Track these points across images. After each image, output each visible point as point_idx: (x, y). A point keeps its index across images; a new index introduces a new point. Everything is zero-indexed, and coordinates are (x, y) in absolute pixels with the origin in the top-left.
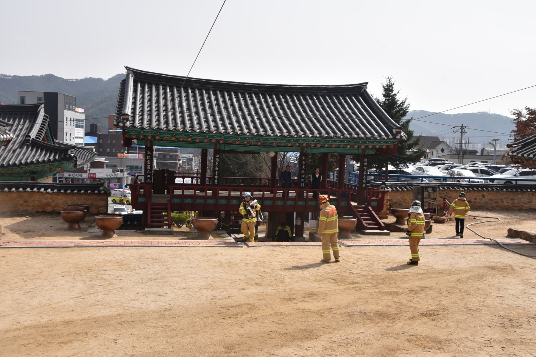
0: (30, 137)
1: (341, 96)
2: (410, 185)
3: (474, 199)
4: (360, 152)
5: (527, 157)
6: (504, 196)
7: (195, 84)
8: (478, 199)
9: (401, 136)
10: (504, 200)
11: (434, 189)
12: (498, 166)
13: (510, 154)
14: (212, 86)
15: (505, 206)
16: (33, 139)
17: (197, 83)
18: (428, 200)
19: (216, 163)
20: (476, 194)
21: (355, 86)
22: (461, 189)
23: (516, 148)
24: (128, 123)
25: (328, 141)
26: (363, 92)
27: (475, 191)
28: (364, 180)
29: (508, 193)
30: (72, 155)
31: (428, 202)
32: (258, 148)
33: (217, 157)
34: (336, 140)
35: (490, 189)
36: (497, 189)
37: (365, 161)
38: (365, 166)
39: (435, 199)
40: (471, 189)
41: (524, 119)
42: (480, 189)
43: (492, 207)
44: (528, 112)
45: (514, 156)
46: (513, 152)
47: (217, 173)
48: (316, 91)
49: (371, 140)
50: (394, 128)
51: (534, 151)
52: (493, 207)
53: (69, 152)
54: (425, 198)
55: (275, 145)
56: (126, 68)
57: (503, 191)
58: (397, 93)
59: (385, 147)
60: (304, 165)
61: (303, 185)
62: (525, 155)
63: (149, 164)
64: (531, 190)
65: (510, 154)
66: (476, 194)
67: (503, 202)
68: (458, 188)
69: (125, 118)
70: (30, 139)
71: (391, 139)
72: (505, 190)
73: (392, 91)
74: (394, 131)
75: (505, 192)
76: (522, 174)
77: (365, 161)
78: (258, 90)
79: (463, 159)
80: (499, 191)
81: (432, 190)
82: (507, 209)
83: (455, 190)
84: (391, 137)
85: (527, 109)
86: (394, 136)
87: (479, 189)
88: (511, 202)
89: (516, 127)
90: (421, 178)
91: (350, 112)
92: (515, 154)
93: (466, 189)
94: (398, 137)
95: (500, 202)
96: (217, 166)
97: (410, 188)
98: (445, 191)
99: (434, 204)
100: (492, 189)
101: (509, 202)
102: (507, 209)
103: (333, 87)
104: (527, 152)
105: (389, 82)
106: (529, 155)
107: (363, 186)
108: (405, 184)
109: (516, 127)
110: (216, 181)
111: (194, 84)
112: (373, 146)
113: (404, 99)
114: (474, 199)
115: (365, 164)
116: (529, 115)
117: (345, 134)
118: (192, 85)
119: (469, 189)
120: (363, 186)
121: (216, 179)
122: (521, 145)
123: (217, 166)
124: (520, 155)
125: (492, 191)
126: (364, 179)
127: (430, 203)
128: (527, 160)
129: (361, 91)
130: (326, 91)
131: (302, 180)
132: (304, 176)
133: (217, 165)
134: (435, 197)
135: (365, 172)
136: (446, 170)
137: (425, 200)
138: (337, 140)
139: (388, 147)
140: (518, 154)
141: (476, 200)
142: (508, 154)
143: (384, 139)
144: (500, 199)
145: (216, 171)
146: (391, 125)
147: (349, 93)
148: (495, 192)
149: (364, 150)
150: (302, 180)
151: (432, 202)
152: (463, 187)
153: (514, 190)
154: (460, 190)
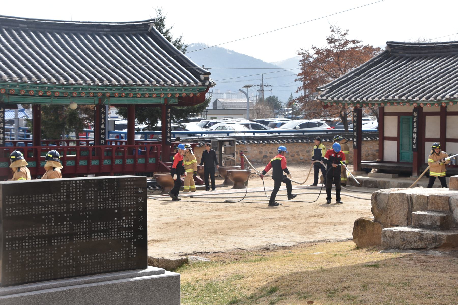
1: (119, 35)
2: (202, 141)
3: (270, 153)
4: (162, 102)
5: (337, 100)
6: (300, 148)
8: (274, 153)
9: (210, 82)
10: (300, 153)
11: (231, 142)
12: (266, 120)
13: (320, 98)
15: (301, 160)
18: (226, 156)
20: (272, 148)
21: (141, 23)
22: (256, 142)
23: (324, 92)
25: (135, 89)
26: (150, 30)
27: (270, 143)
28: (169, 133)
29: (303, 144)
31: (226, 158)
32: (49, 100)
34: (143, 88)
35: (286, 141)
36: (292, 141)
37: (168, 112)
38: (168, 117)
39: (234, 154)
40: (266, 142)
41: (311, 60)
42: (276, 141)
43: (288, 161)
44: (315, 52)
45: (323, 99)
46: (322, 96)
48: (97, 30)
49: (180, 88)
50: (201, 74)
51: (342, 94)
52: (290, 161)
54: (223, 154)
55: (85, 96)
57: (299, 143)
58: (170, 29)
59: (191, 95)
60: (103, 118)
61: (104, 142)
62: (335, 99)
64: (326, 140)
65: (320, 98)
66: (272, 147)
67: (298, 155)
68: (253, 142)
71: (200, 86)
72: (300, 141)
73: (163, 26)
74: (202, 77)
75: (300, 144)
76: (302, 126)
77: (168, 112)
78: (26, 26)
79: (207, 115)
80: (294, 142)
81: (230, 144)
82: (303, 162)
83: (251, 144)
84: (200, 83)
85: (313, 48)
86: (203, 82)
87: (274, 142)
88: (307, 154)
89: (302, 69)
90: (200, 135)
91: (145, 56)
92: (324, 98)
93: (261, 142)
94: (207, 84)
95: (296, 156)
97: (203, 144)
98: (240, 145)
99: (233, 159)
100: (288, 141)
101: (304, 154)
102: (303, 162)
103: (117, 24)
104: (336, 95)
105: (159, 15)
106: (338, 98)
107: (168, 141)
108: (197, 139)
109: (302, 69)
112: (180, 94)
113: (180, 37)
114: (270, 153)
115: (168, 115)
116: (315, 56)
117: (191, 82)
119: (264, 142)
120: (168, 141)
122: (329, 88)
124: (329, 98)
125: (287, 143)
126: (168, 132)
127: (228, 159)
128: (337, 104)
129: (148, 30)
130: (109, 30)
131: (102, 136)
132: (103, 131)
134: (233, 153)
135: (169, 124)
136: (203, 127)
137: (224, 156)
138: (145, 89)
139: (195, 95)
140: (327, 97)
141: (271, 155)
142: (317, 99)
143: (193, 86)
144: (296, 152)
146: (198, 71)
147: (135, 32)
148: (290, 144)
149: (166, 100)
150: (102, 136)
151: (230, 157)
152: (257, 140)
153: (310, 141)
154: (255, 143)
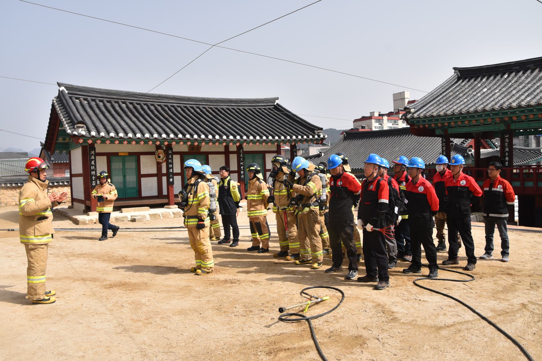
0: (453, 142)
7: (514, 67)
14: (533, 65)
16: (455, 143)
17: (516, 66)
19: (506, 144)
24: (410, 115)
30: (470, 153)
33: (506, 138)
47: (507, 154)
53: (468, 150)
56: (455, 69)
63: (444, 151)
69: (408, 111)
70: (453, 144)
96: (507, 147)
110: (507, 163)
111: (514, 68)
118: (512, 69)
121: (506, 161)
123: (507, 147)
133: (507, 146)
145: (506, 152)
